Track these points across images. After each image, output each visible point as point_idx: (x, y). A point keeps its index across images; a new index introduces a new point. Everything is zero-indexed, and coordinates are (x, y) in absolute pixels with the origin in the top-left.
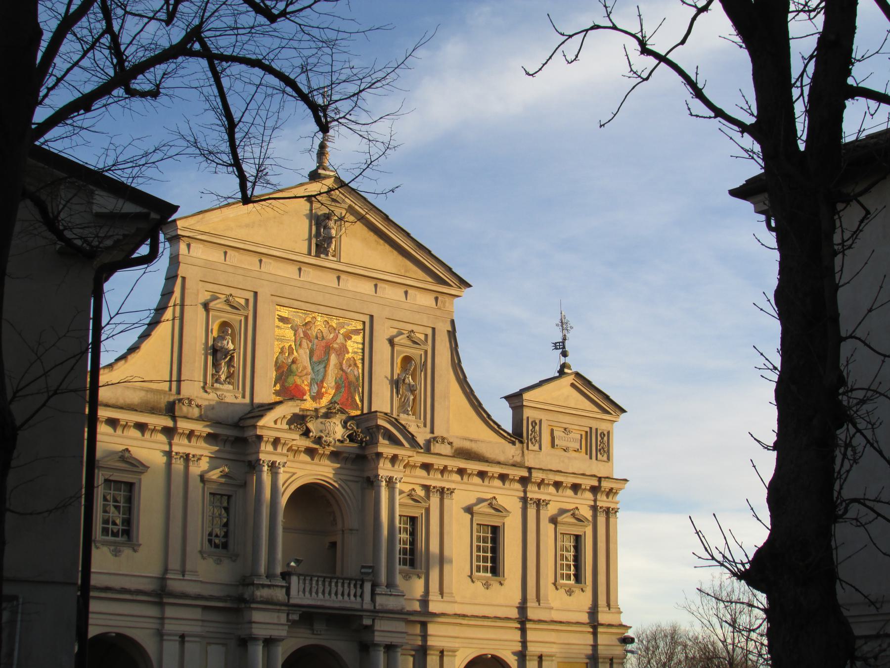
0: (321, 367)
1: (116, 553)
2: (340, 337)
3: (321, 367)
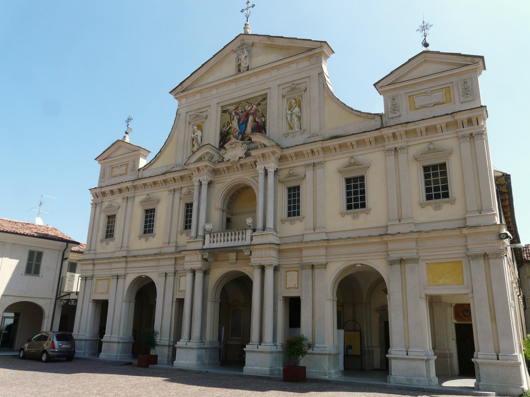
0: (244, 126)
1: (147, 240)
2: (255, 106)
3: (244, 126)
